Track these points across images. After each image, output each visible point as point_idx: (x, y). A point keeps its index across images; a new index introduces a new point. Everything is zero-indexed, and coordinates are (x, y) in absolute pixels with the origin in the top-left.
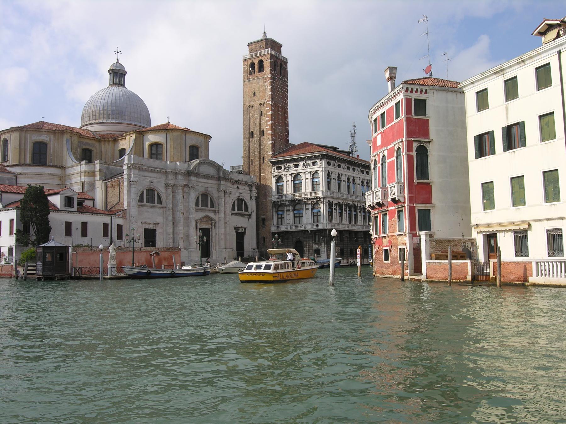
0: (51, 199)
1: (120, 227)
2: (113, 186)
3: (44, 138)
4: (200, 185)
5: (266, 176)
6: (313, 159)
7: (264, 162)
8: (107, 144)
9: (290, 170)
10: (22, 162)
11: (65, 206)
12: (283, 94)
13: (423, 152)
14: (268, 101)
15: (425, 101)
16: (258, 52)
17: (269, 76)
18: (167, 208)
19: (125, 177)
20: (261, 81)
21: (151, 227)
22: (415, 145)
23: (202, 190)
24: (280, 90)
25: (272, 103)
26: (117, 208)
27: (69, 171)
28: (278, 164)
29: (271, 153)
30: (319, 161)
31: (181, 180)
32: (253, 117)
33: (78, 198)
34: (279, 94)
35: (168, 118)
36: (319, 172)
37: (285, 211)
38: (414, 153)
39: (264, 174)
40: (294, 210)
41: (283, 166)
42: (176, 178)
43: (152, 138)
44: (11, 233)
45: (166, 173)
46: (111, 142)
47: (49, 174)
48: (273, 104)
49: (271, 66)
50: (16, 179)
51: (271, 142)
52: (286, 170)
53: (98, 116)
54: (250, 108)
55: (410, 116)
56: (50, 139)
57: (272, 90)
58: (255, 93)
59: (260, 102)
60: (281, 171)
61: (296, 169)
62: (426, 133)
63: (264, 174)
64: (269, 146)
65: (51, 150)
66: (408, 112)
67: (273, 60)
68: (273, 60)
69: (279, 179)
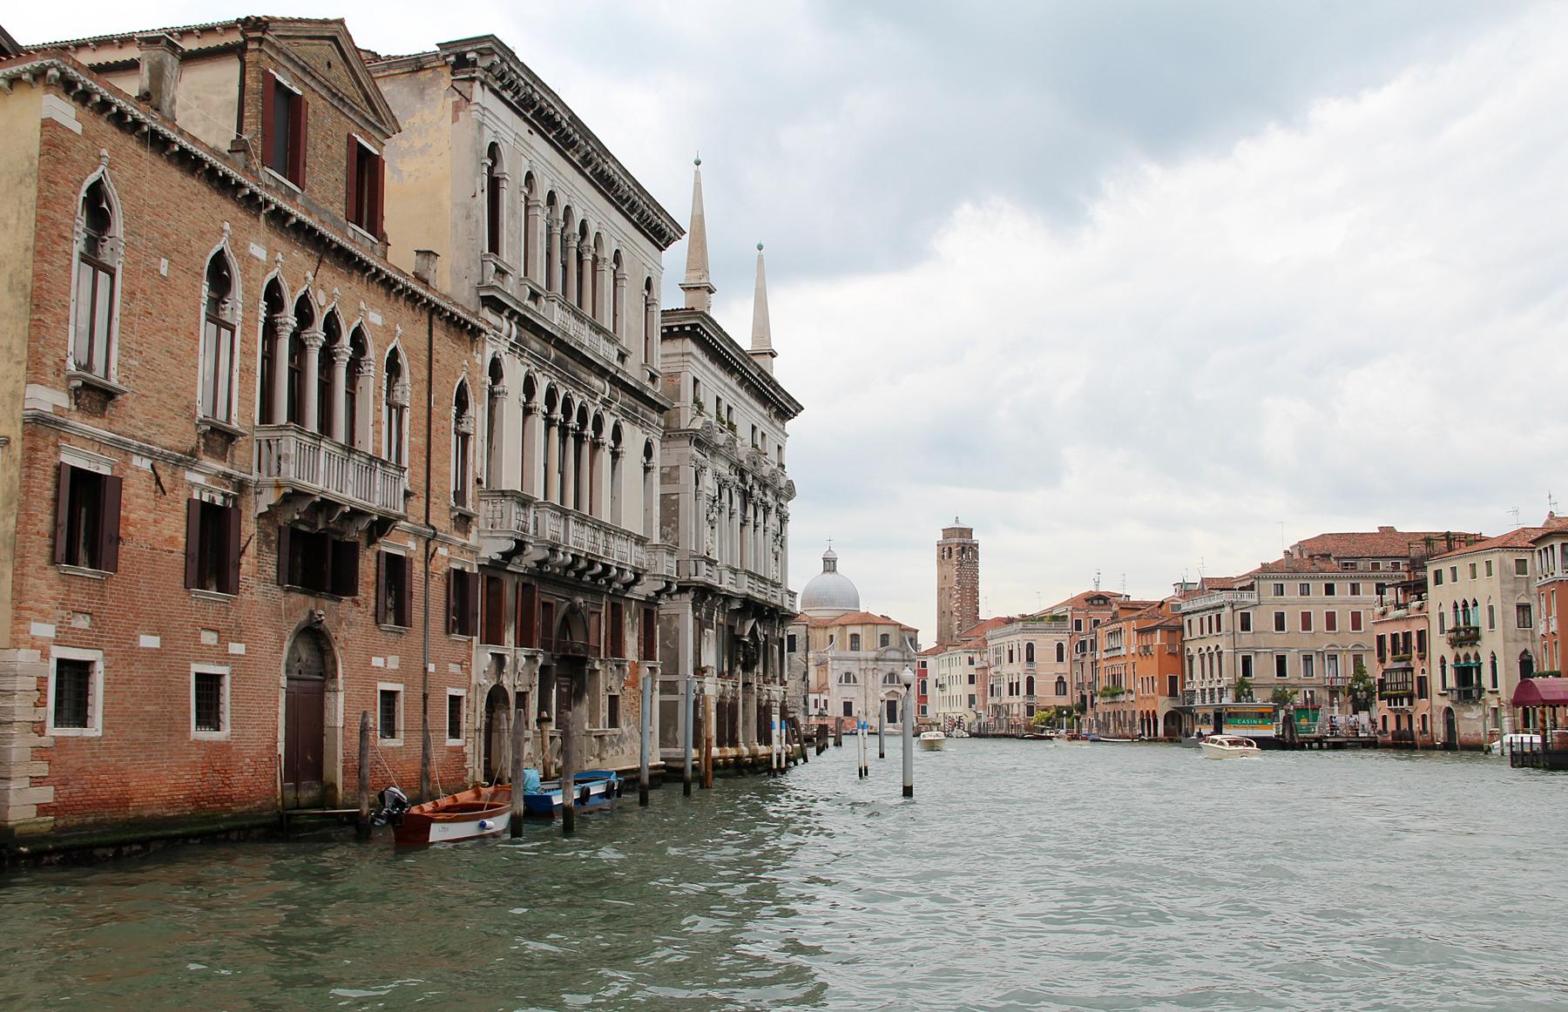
1: (826, 701)
4: (888, 668)
13: (924, 683)
19: (829, 666)
21: (848, 700)
23: (889, 670)
31: (871, 665)
43: (851, 630)
45: (859, 660)
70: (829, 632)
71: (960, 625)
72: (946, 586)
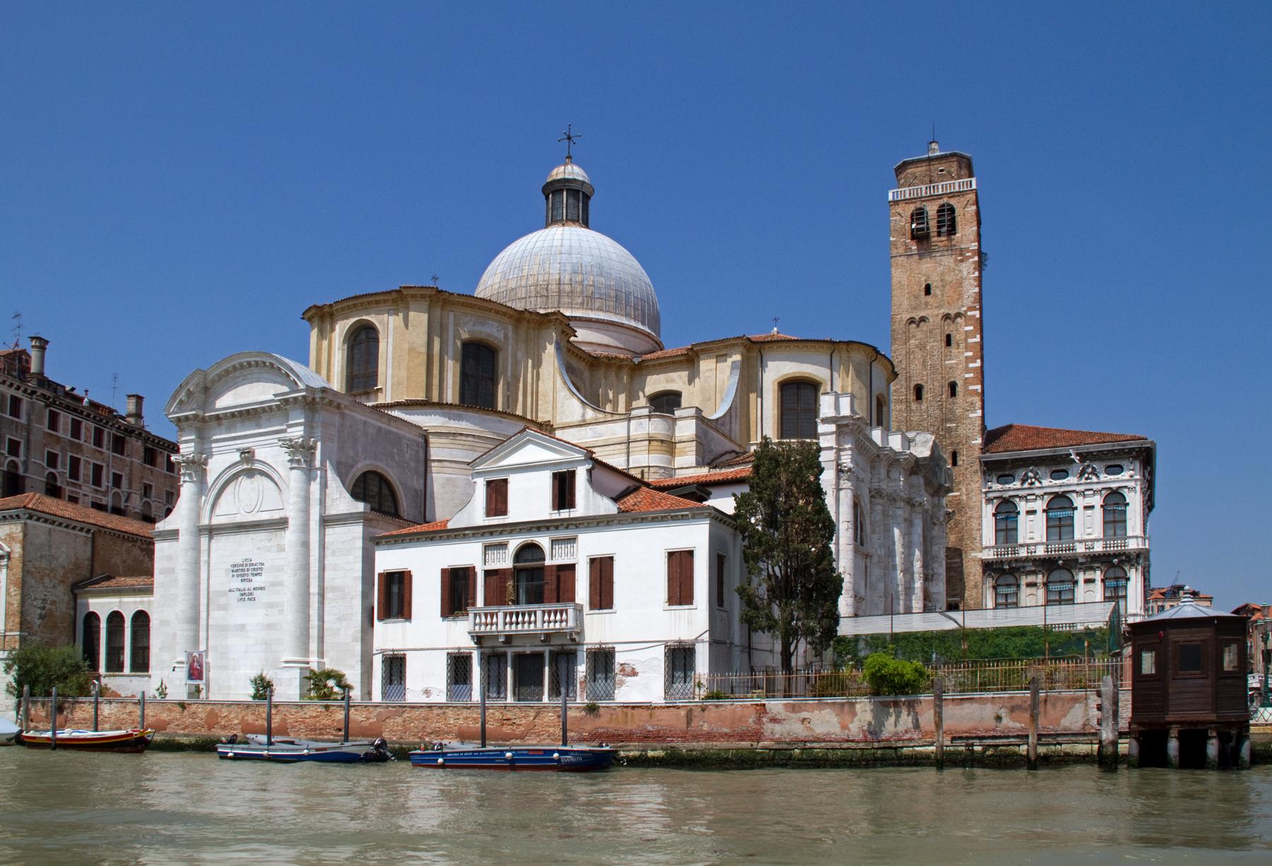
3: (493, 331)
5: (964, 497)
6: (1109, 460)
7: (955, 463)
9: (1037, 484)
10: (435, 399)
18: (875, 559)
28: (996, 469)
29: (979, 441)
30: (1124, 463)
36: (1125, 492)
39: (958, 494)
41: (1021, 473)
42: (889, 477)
46: (625, 371)
50: (424, 446)
52: (1026, 485)
53: (556, 298)
56: (506, 337)
60: (1011, 486)
63: (958, 494)
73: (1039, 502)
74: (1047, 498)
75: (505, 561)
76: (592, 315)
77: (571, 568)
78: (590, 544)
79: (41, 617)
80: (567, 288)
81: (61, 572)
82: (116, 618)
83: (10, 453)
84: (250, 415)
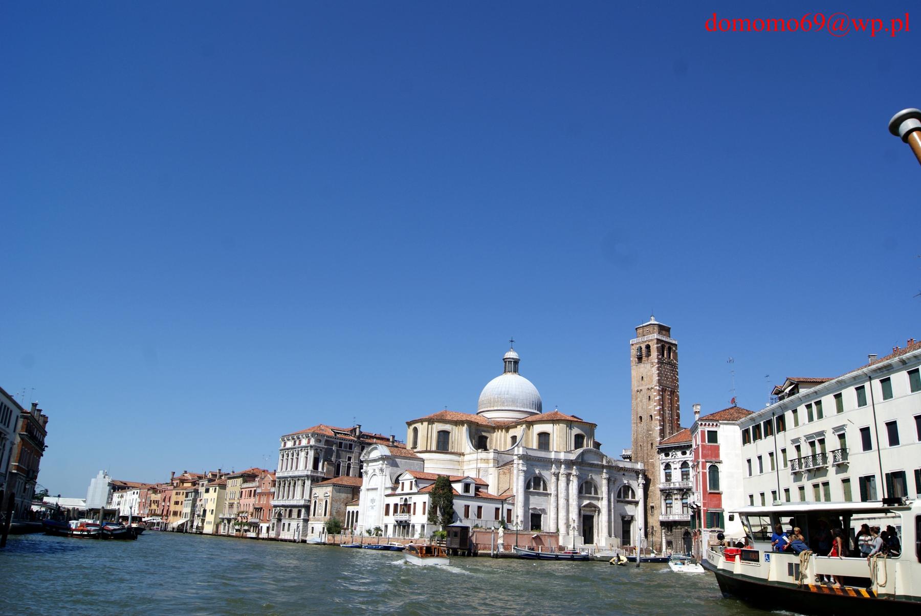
0: (454, 485)
2: (504, 473)
3: (447, 427)
8: (500, 430)
10: (429, 449)
11: (464, 492)
12: (672, 378)
14: (656, 386)
15: (716, 432)
16: (645, 337)
17: (656, 361)
19: (515, 466)
20: (648, 366)
22: (708, 465)
24: (669, 374)
25: (660, 388)
26: (508, 493)
27: (466, 458)
28: (666, 451)
32: (641, 401)
33: (476, 484)
34: (667, 378)
35: (557, 406)
37: (674, 500)
38: (707, 471)
40: (682, 499)
44: (424, 513)
47: (451, 460)
48: (660, 389)
49: (658, 351)
51: (659, 428)
52: (673, 457)
54: (638, 393)
55: (704, 444)
56: (452, 429)
57: (659, 375)
58: (642, 377)
59: (647, 387)
61: (684, 456)
62: (717, 455)
64: (657, 432)
65: (452, 437)
66: (703, 440)
67: (660, 345)
68: (660, 345)
69: (668, 466)
70: (512, 432)
71: (660, 429)
72: (644, 388)
73: (678, 464)
74: (681, 463)
75: (403, 503)
76: (503, 408)
77: (410, 504)
78: (415, 499)
79: (336, 512)
80: (497, 400)
81: (342, 499)
82: (353, 512)
83: (348, 460)
84: (375, 460)
